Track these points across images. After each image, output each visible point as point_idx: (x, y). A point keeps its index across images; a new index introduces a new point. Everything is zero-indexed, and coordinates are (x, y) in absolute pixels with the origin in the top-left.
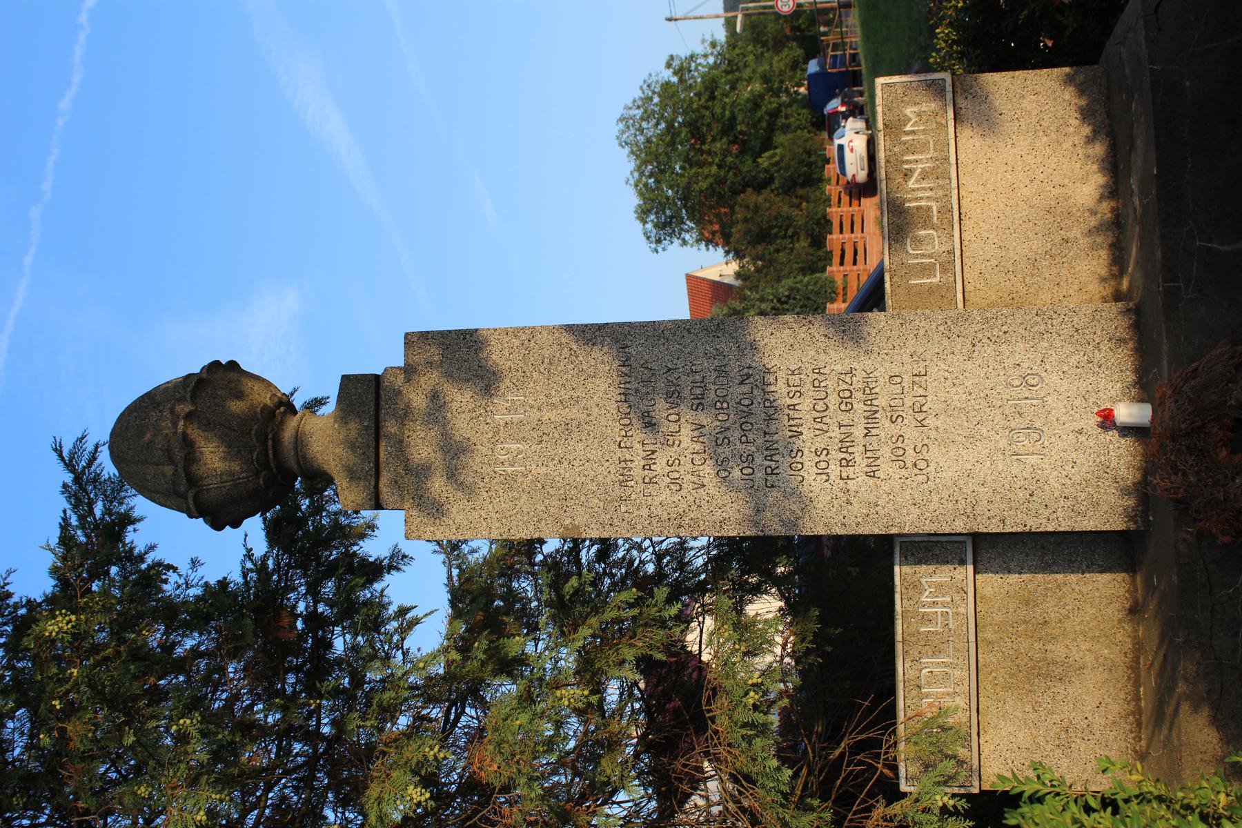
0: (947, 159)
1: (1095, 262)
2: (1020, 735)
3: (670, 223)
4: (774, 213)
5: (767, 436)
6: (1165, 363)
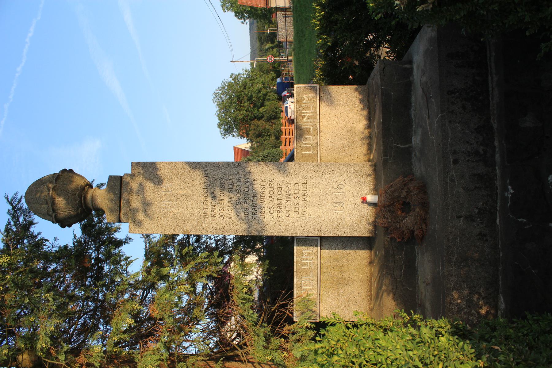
0: (316, 113)
1: (362, 149)
2: (333, 303)
3: (229, 129)
4: (264, 128)
5: (253, 202)
6: (383, 183)
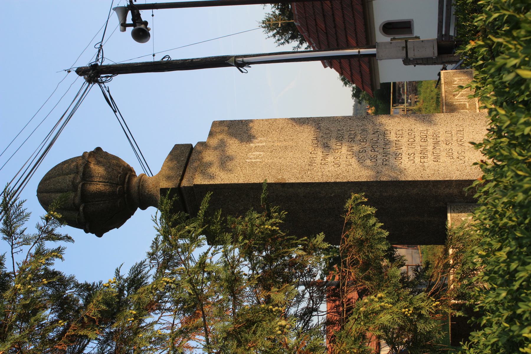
5: (385, 150)
